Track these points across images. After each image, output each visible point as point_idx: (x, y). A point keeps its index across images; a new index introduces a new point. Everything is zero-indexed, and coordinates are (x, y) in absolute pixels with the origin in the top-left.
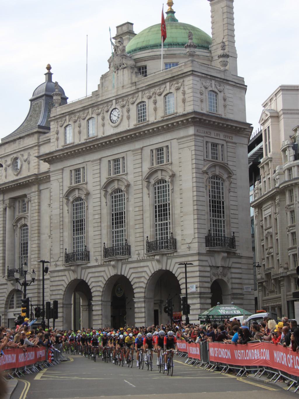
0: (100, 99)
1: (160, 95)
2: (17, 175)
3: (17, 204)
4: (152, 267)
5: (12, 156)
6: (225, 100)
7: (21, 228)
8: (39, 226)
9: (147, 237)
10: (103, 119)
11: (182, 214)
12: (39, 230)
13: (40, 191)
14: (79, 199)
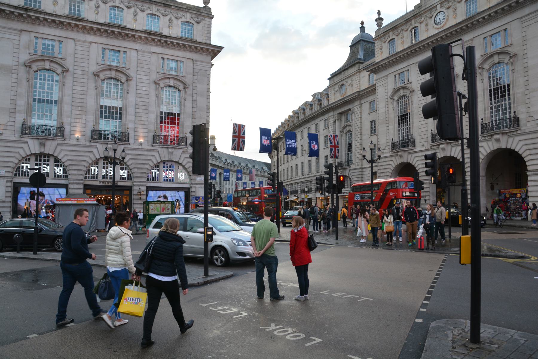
0: (423, 9)
3: (343, 118)
7: (346, 133)
8: (361, 130)
9: (482, 119)
11: (527, 92)
12: (361, 132)
13: (361, 104)
14: (404, 96)
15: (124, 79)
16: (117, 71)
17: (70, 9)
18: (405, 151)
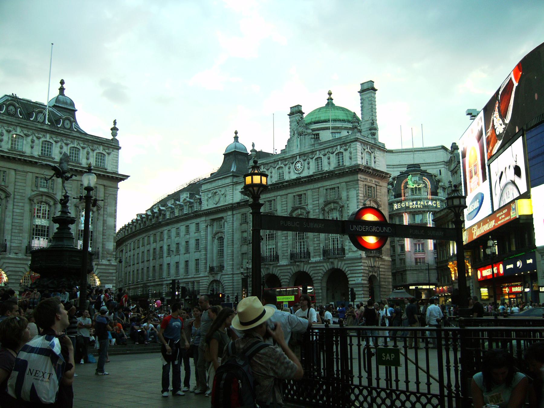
1: (333, 153)
2: (216, 204)
3: (215, 224)
4: (327, 266)
5: (212, 191)
6: (375, 158)
7: (218, 239)
10: (289, 168)
13: (233, 215)
15: (52, 203)
16: (47, 196)
17: (12, 144)
18: (271, 265)
